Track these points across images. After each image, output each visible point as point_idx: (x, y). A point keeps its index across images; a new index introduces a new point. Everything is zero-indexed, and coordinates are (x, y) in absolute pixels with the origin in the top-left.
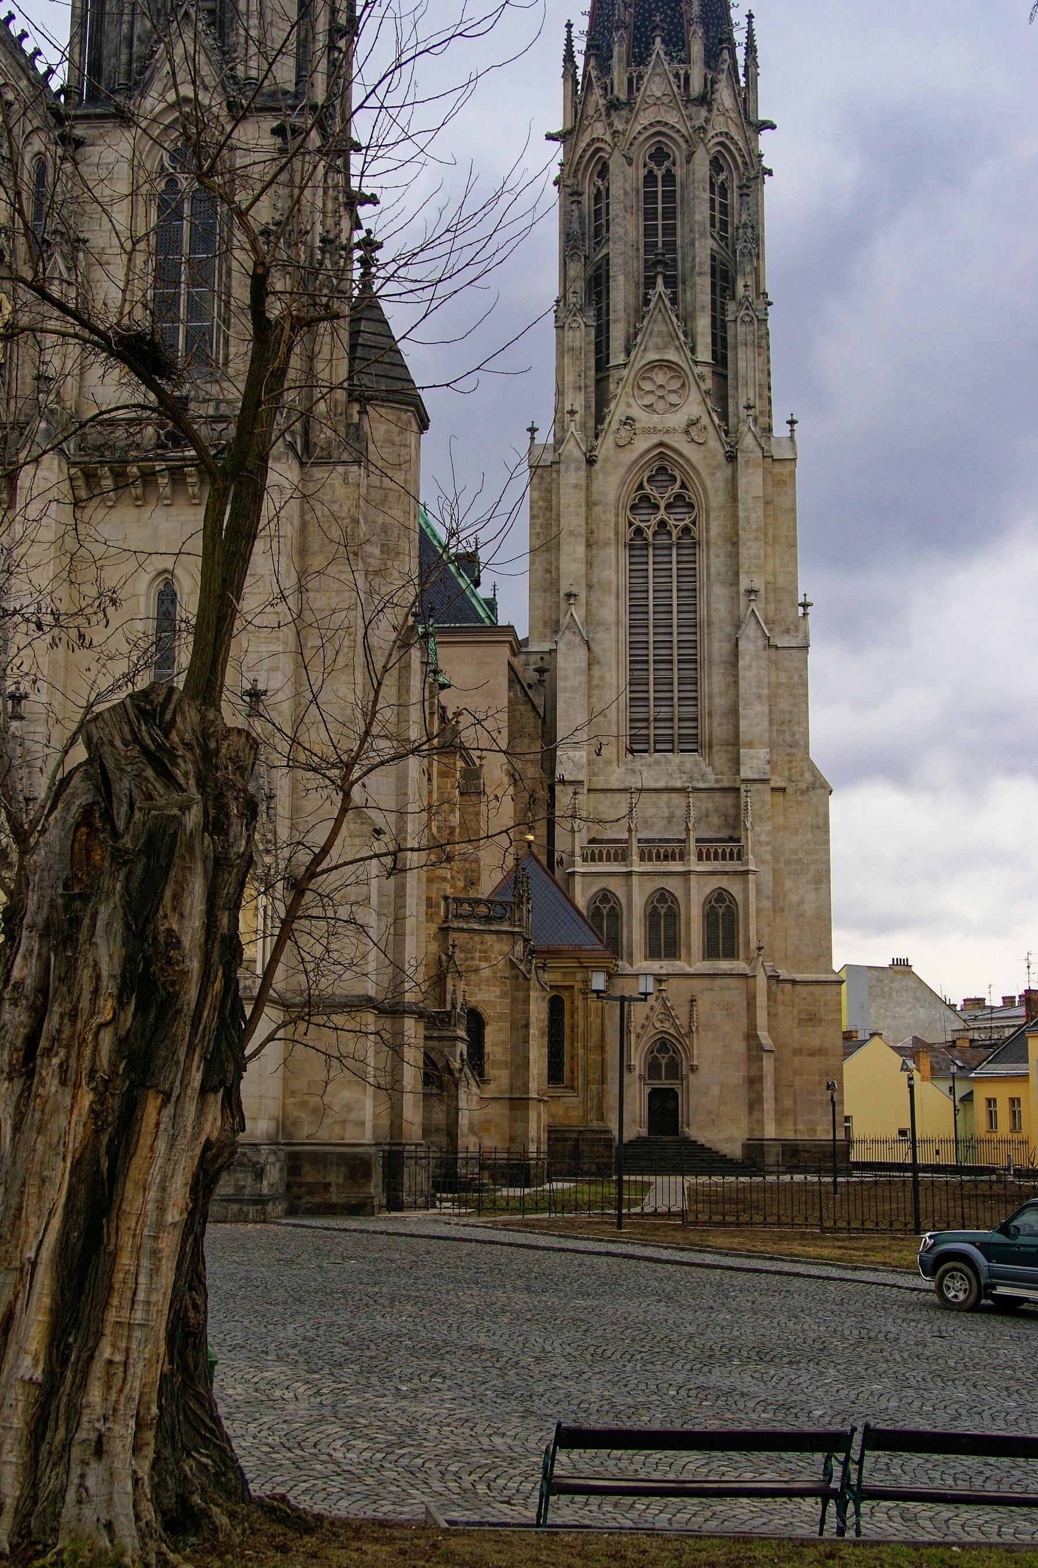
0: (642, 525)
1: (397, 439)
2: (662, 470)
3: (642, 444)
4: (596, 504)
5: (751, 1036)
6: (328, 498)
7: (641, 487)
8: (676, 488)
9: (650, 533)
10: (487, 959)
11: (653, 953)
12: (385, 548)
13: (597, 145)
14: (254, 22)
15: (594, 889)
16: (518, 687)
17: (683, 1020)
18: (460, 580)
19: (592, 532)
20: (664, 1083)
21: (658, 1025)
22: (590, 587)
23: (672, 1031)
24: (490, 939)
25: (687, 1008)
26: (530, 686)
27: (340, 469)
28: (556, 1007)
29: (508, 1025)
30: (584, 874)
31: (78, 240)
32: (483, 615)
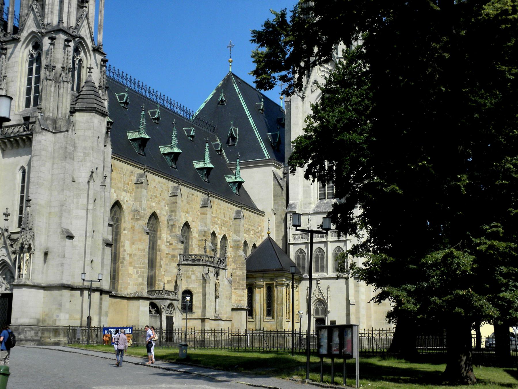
1: (89, 121)
5: (348, 299)
10: (194, 274)
11: (317, 271)
12: (85, 153)
14: (50, 7)
17: (325, 295)
20: (321, 316)
23: (322, 298)
26: (281, 179)
27: (63, 133)
29: (201, 295)
30: (294, 244)
32: (266, 155)
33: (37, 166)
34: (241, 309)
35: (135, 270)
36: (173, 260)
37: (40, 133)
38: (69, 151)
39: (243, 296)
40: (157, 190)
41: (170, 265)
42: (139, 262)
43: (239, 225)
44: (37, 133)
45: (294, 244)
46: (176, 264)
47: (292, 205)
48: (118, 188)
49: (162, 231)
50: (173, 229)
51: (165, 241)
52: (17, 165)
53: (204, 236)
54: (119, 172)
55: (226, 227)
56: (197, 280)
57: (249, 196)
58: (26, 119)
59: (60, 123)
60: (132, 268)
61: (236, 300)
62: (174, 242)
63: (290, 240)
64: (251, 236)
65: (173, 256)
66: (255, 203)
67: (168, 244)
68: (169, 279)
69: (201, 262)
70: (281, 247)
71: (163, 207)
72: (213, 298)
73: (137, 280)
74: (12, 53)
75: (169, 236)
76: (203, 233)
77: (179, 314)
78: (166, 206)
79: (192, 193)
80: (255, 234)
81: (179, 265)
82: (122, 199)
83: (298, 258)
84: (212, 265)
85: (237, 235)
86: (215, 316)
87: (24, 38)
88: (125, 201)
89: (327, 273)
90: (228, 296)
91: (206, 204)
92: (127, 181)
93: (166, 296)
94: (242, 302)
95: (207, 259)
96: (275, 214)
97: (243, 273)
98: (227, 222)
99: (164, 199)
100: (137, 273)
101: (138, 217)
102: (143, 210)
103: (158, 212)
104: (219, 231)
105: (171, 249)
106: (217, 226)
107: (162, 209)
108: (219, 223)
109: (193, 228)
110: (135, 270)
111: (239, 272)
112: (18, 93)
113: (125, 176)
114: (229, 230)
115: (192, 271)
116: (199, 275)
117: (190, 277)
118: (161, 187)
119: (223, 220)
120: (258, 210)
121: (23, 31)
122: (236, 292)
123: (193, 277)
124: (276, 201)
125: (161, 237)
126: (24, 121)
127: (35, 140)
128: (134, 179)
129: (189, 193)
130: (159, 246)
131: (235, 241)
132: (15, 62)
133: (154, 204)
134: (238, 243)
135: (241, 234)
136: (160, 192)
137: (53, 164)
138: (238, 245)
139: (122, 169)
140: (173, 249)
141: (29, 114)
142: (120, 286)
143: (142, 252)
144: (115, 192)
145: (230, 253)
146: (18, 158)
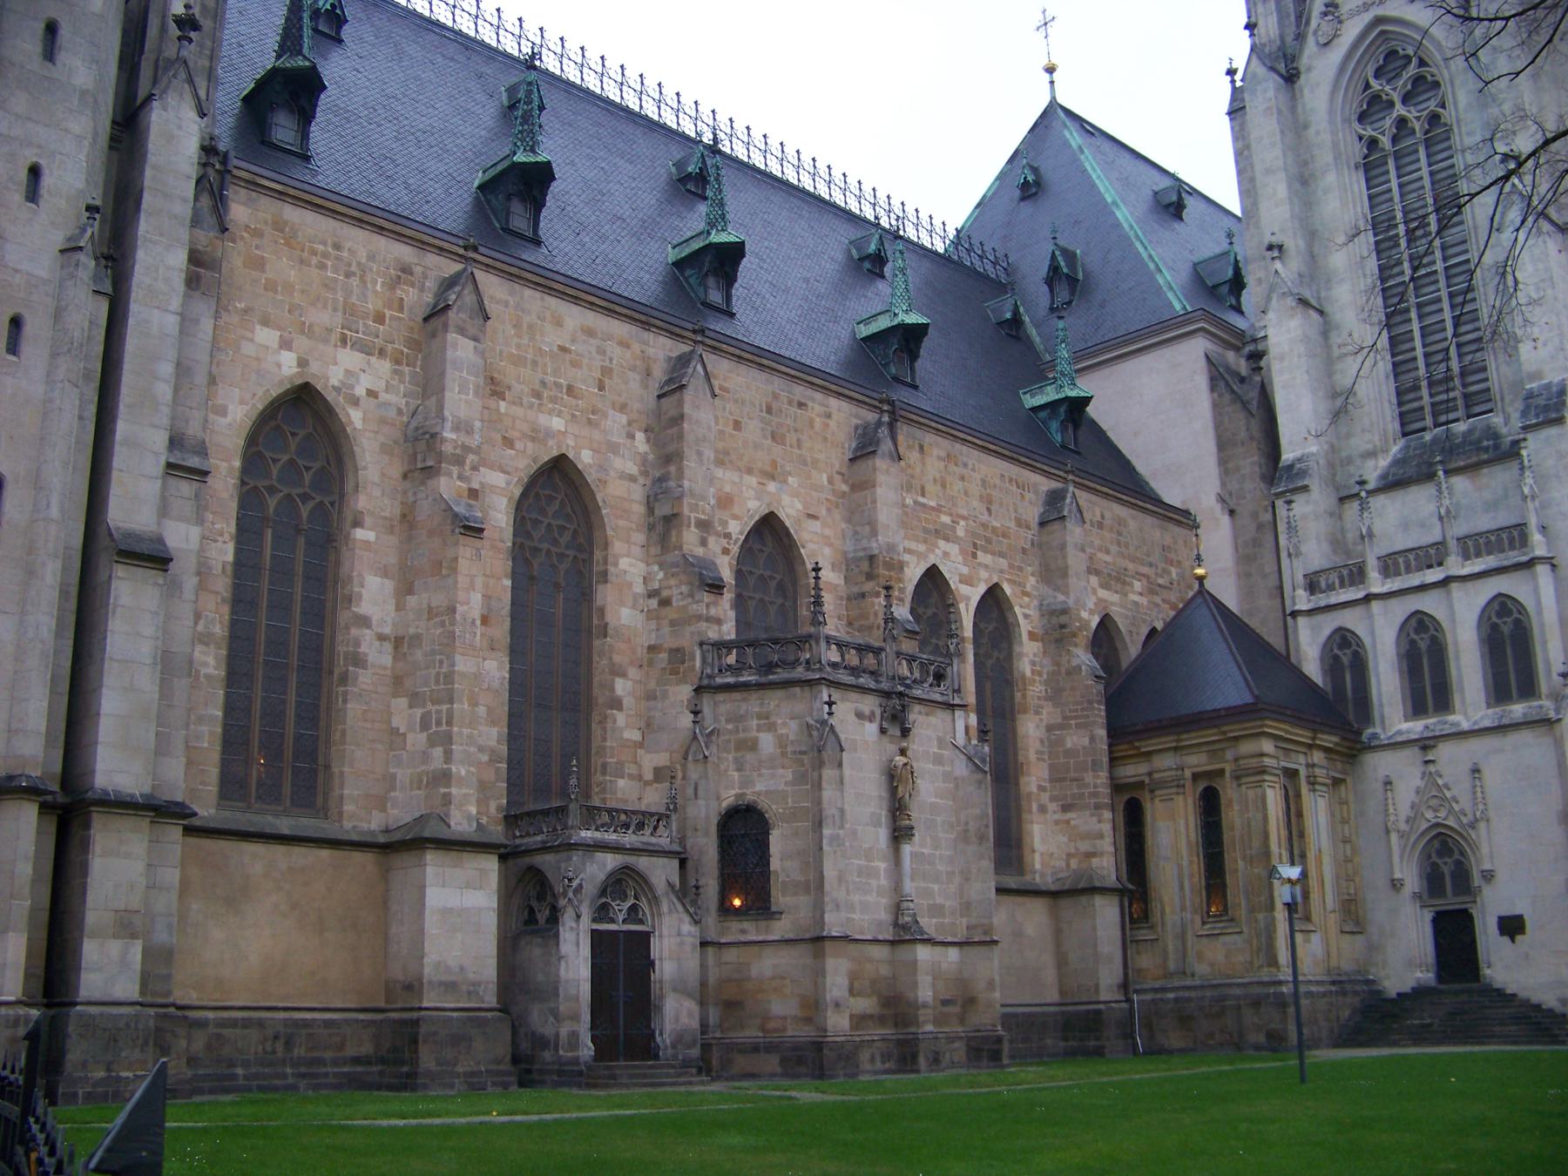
0: (1374, 133)
2: (1391, 55)
3: (1352, 30)
4: (1306, 127)
7: (1367, 86)
8: (1412, 70)
9: (1385, 141)
10: (771, 727)
11: (1417, 708)
15: (1327, 632)
16: (1222, 384)
17: (1465, 803)
18: (1158, 277)
19: (1306, 163)
20: (1451, 902)
21: (1429, 815)
22: (1312, 235)
23: (1451, 822)
24: (774, 699)
25: (1467, 785)
28: (1210, 804)
30: (1310, 612)
34: (1092, 890)
35: (419, 712)
36: (674, 672)
39: (1101, 836)
40: (576, 364)
41: (665, 695)
42: (433, 672)
43: (1063, 547)
45: (1310, 612)
46: (685, 692)
47: (1291, 467)
48: (306, 330)
49: (618, 547)
50: (674, 533)
51: (639, 588)
53: (870, 576)
54: (314, 260)
55: (1002, 555)
56: (784, 754)
57: (1128, 462)
60: (403, 702)
61: (1069, 855)
62: (677, 590)
63: (1293, 598)
64: (1134, 597)
65: (678, 655)
66: (1153, 484)
67: (654, 603)
68: (662, 759)
69: (800, 669)
70: (1320, 683)
71: (618, 438)
72: (882, 835)
73: (425, 757)
75: (656, 568)
76: (865, 566)
77: (681, 920)
78: (640, 436)
79: (797, 397)
80: (1152, 592)
81: (699, 690)
82: (334, 381)
83: (1332, 665)
84: (864, 680)
85: (1057, 589)
86: (896, 924)
88: (360, 391)
89: (1465, 714)
90: (972, 827)
91: (870, 444)
92: (371, 305)
93: (583, 834)
94: (1095, 862)
95: (833, 655)
96: (1232, 512)
97: (1092, 739)
98: (1004, 536)
99: (623, 408)
100: (425, 725)
101: (430, 464)
102: (456, 428)
103: (585, 459)
104: (965, 570)
105: (666, 622)
106: (953, 549)
107: (614, 448)
108: (960, 533)
109: (811, 546)
110: (419, 712)
111: (1075, 738)
113: (355, 281)
114: (1020, 569)
115: (759, 717)
116: (791, 729)
117: (753, 746)
118: (602, 352)
119: (984, 526)
120: (1158, 501)
122: (1068, 822)
123: (767, 742)
124: (1230, 465)
125: (611, 569)
128: (417, 298)
129: (776, 396)
130: (602, 610)
131: (1053, 613)
133: (557, 424)
134: (1063, 619)
135: (1072, 581)
136: (597, 374)
138: (1063, 627)
139: (337, 247)
140: (673, 623)
142: (336, 793)
143: (442, 624)
144: (286, 344)
145: (1033, 663)
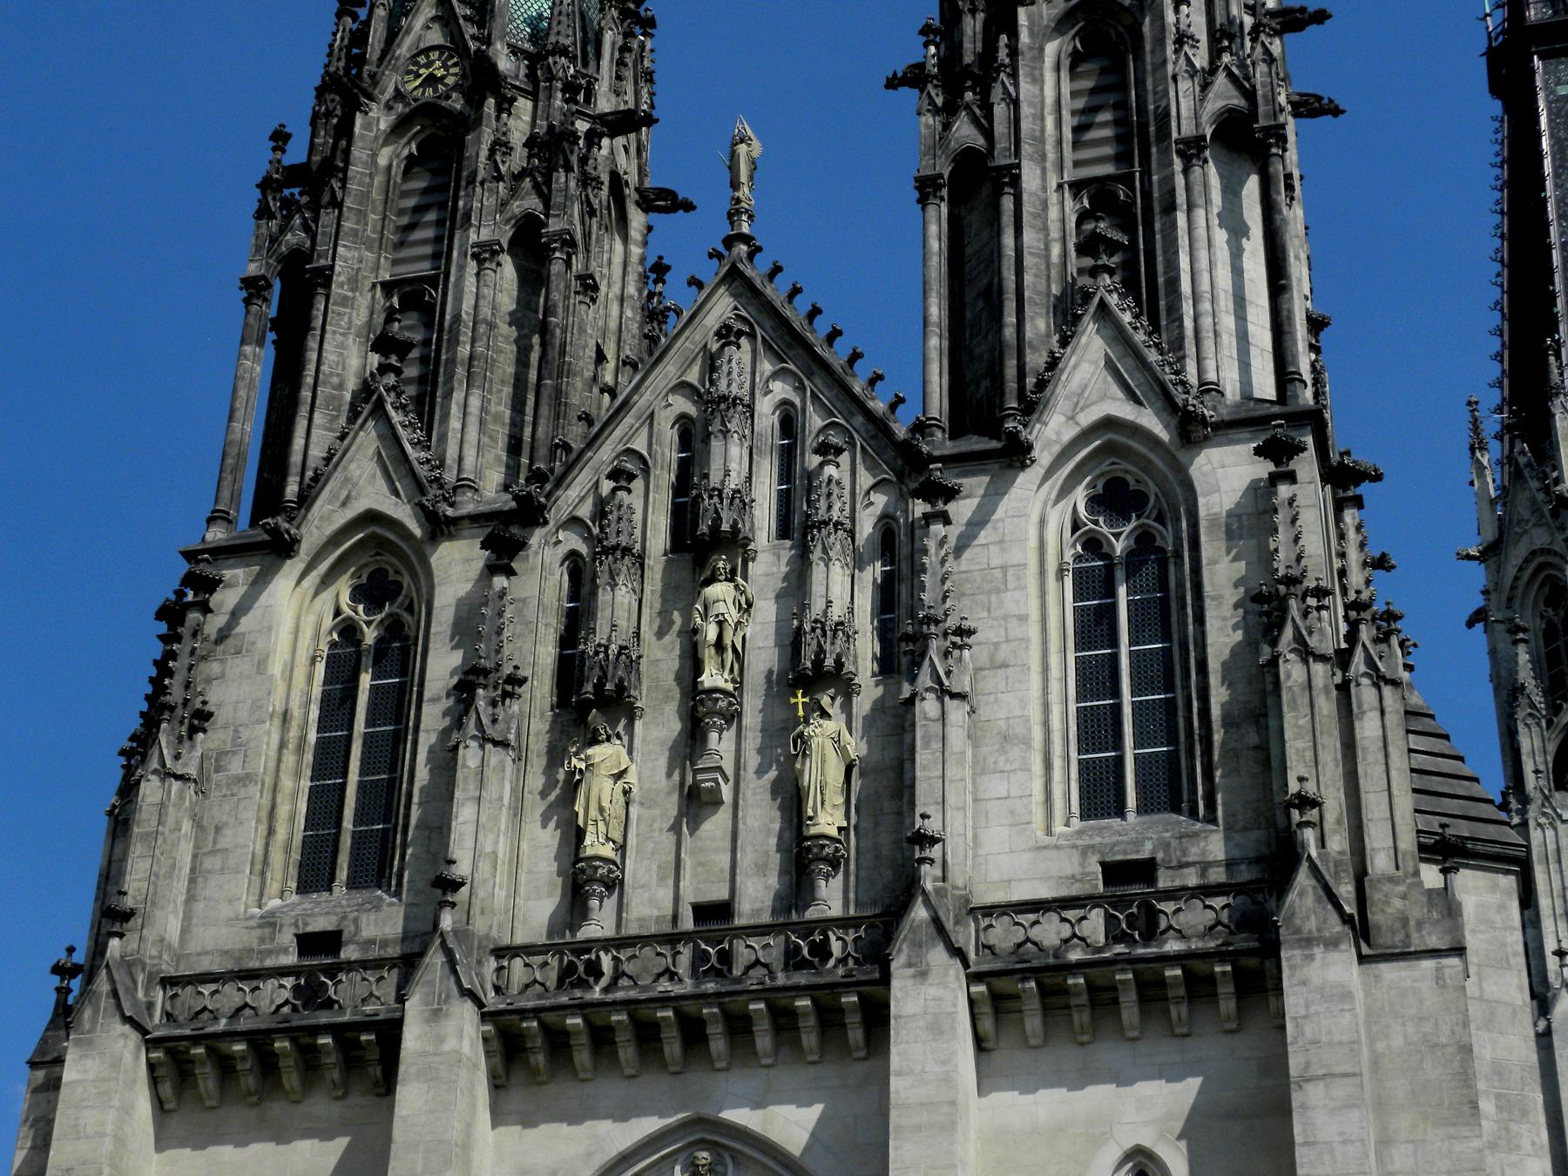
1: (1497, 918)
6: (1413, 1011)
13: (1541, 559)
27: (1428, 964)
31: (961, 632)
33: (1344, 1142)
37: (1332, 944)
38: (1499, 1069)
44: (1308, 942)
52: (1096, 1142)
58: (1115, 872)
59: (1397, 903)
74: (978, 522)
87: (1057, 449)
112: (1037, 734)
121: (1044, 417)
126: (1106, 884)
127: (1304, 983)
132: (1004, 568)
137: (1385, 1142)
141: (1148, 846)
146: (1099, 1095)
